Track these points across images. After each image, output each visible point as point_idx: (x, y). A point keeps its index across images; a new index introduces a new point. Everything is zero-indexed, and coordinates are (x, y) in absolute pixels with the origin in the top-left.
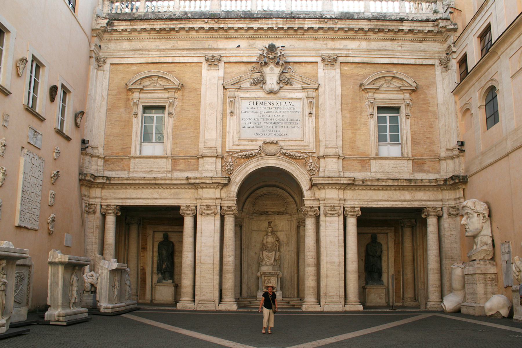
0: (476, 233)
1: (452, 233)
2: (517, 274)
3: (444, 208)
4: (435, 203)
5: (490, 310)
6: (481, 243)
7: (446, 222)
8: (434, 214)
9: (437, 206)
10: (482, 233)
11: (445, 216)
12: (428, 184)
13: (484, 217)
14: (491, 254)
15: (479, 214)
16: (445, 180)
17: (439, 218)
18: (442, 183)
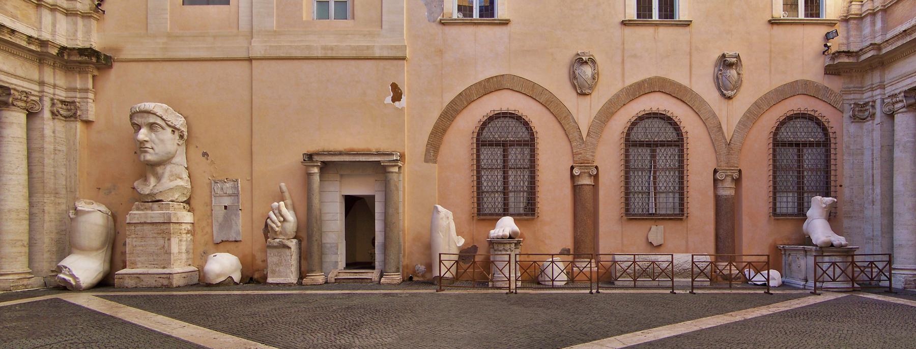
0: (165, 158)
1: (59, 148)
2: (279, 224)
3: (45, 98)
4: (26, 84)
5: (219, 275)
6: (172, 175)
7: (49, 127)
8: (23, 104)
9: (33, 93)
10: (174, 161)
11: (47, 114)
12: (24, 44)
13: (181, 137)
14: (188, 194)
15: (174, 129)
16: (63, 49)
17: (31, 115)
18: (54, 51)
